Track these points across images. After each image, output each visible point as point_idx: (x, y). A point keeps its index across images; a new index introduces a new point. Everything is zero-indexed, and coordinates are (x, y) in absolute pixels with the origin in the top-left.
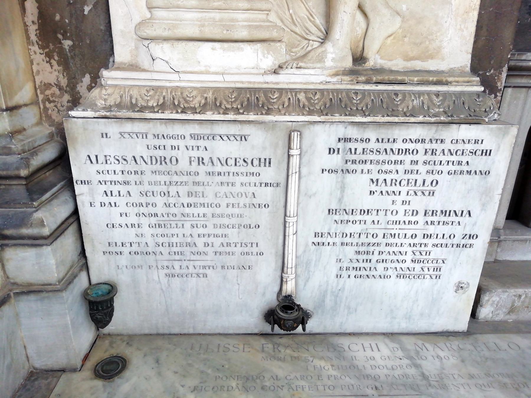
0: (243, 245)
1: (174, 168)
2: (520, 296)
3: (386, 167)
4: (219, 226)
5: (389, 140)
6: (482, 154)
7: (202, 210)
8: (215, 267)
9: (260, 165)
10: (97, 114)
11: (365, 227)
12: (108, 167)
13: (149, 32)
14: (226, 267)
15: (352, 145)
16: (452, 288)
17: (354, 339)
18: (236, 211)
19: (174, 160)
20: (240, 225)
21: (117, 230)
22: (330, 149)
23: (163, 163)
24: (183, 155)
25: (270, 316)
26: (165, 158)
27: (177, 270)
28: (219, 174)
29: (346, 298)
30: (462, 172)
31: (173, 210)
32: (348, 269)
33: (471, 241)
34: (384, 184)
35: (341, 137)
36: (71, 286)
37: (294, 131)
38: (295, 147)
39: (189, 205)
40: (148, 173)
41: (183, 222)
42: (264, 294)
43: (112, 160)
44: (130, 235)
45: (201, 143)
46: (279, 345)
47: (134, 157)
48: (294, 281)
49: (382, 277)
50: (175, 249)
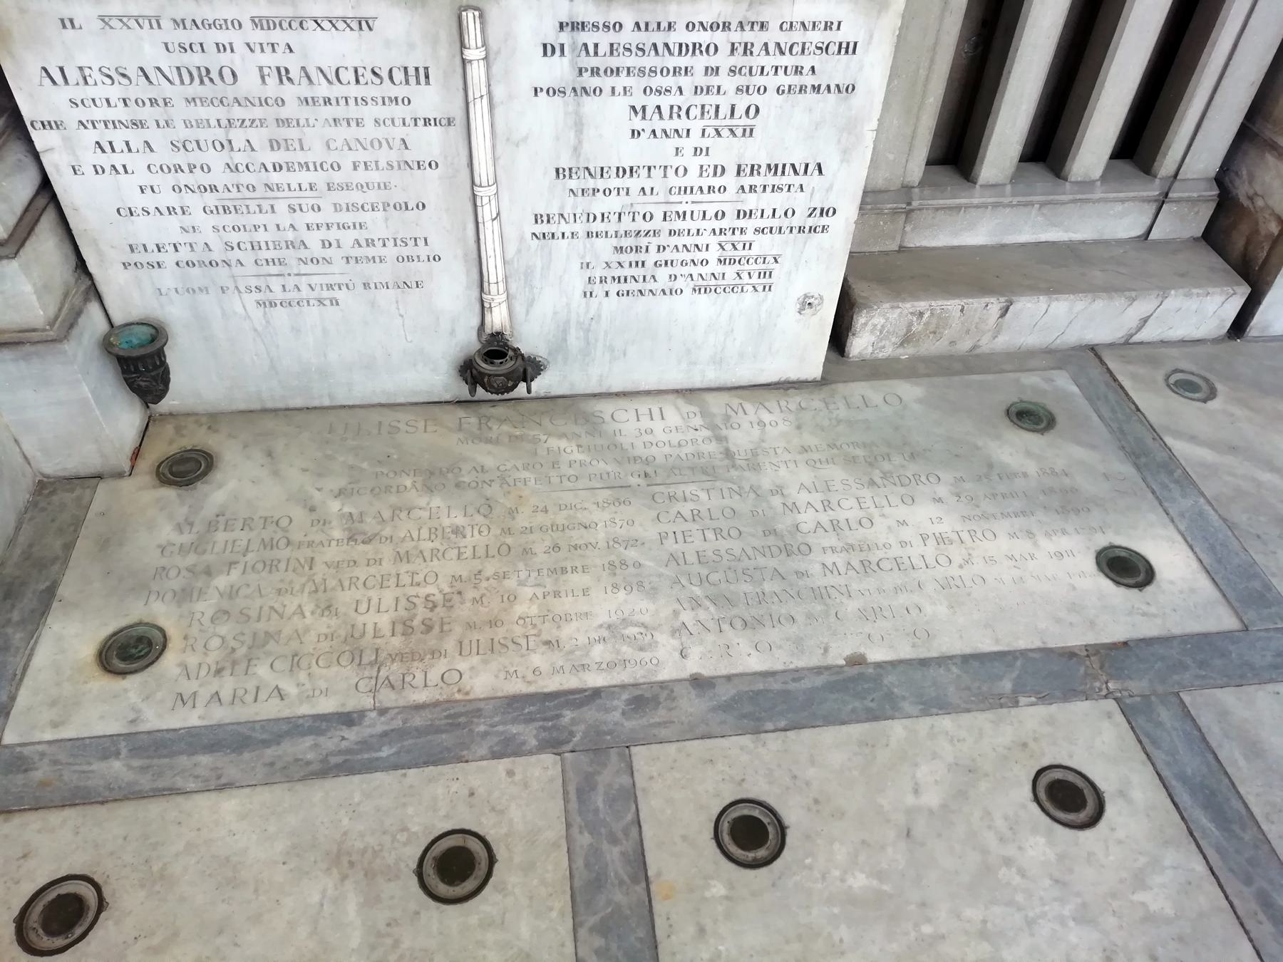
0: (399, 242)
1: (230, 92)
2: (921, 314)
3: (658, 81)
4: (344, 207)
5: (659, 24)
6: (839, 51)
7: (305, 177)
8: (351, 286)
9: (407, 82)
11: (627, 200)
12: (90, 92)
14: (372, 286)
15: (589, 37)
16: (793, 307)
17: (622, 403)
18: (375, 176)
20: (386, 206)
21: (141, 221)
22: (545, 46)
23: (206, 80)
24: (246, 65)
25: (469, 371)
26: (208, 71)
27: (278, 294)
28: (327, 101)
29: (606, 332)
30: (802, 89)
31: (246, 178)
32: (603, 280)
33: (825, 221)
34: (657, 116)
35: (565, 20)
36: (75, 332)
37: (467, 8)
38: (473, 43)
39: (277, 167)
40: (179, 103)
41: (271, 202)
42: (453, 332)
44: (170, 229)
45: (277, 36)
46: (489, 419)
47: (142, 69)
48: (504, 306)
49: (668, 292)
50: (265, 254)
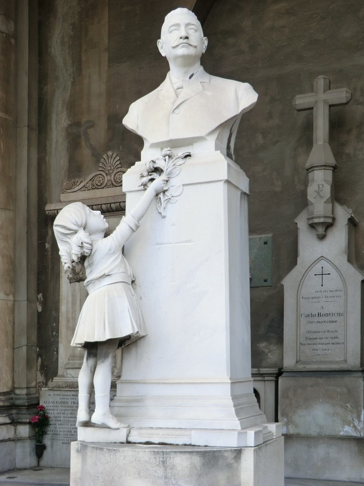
10: (49, 389)
19: (67, 402)
27: (65, 441)
31: (66, 419)
40: (60, 407)
43: (51, 402)
50: (65, 433)
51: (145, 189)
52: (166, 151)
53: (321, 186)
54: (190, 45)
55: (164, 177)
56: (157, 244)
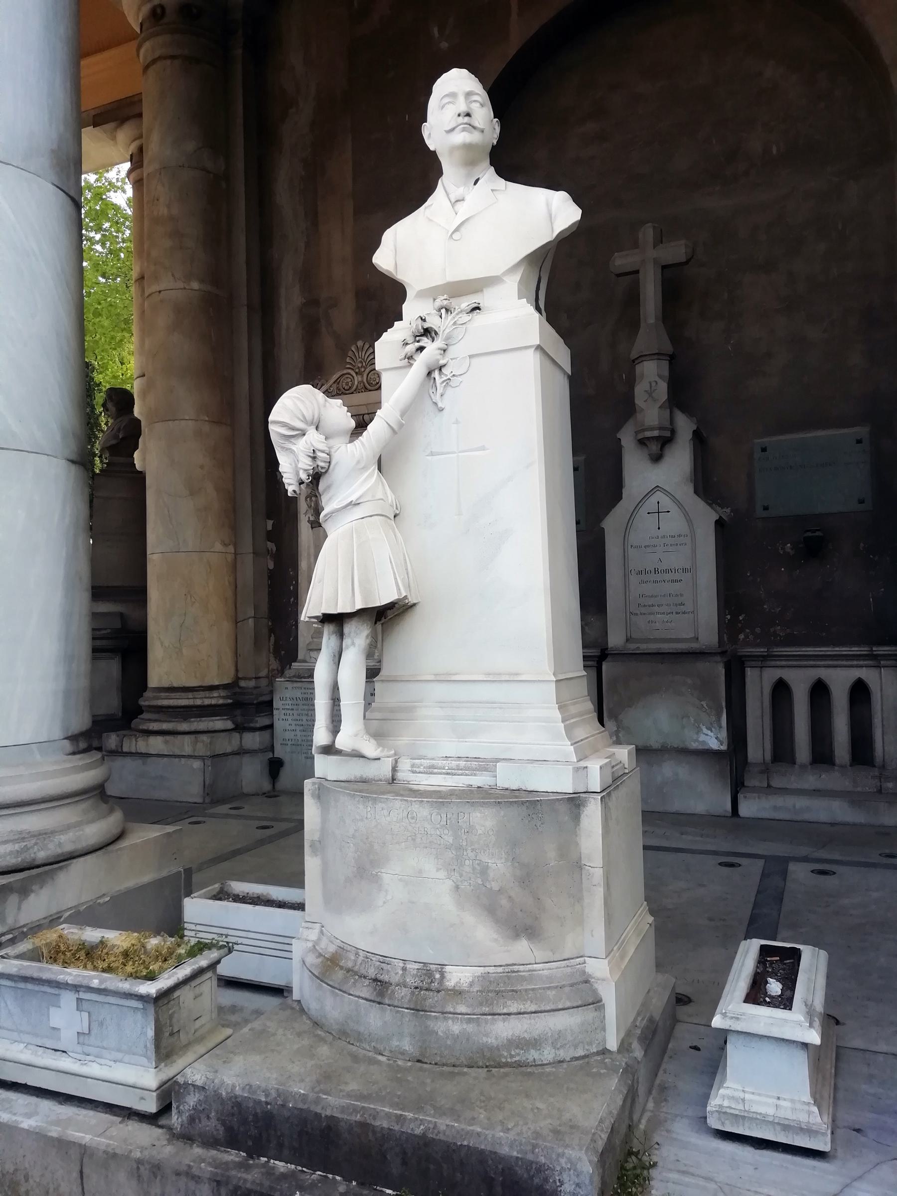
13: (310, 648)
51: (411, 365)
52: (441, 301)
53: (654, 384)
54: (474, 127)
55: (439, 343)
56: (432, 454)
